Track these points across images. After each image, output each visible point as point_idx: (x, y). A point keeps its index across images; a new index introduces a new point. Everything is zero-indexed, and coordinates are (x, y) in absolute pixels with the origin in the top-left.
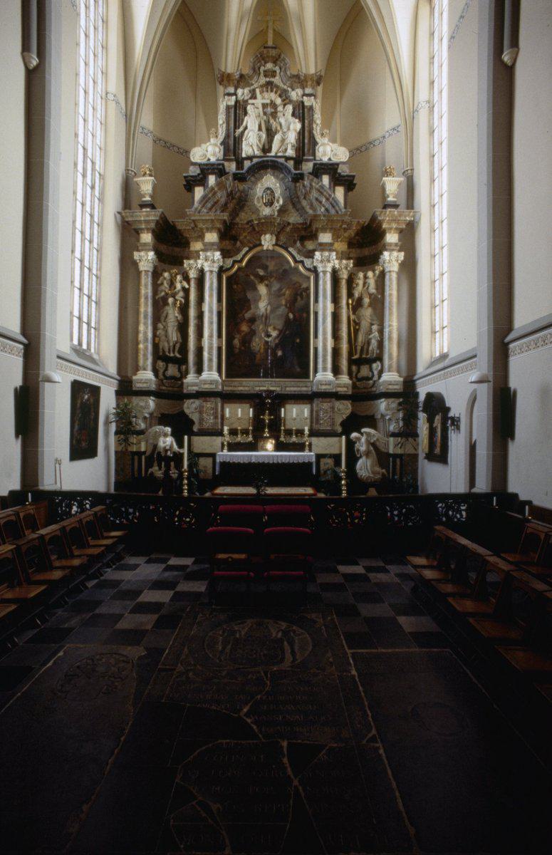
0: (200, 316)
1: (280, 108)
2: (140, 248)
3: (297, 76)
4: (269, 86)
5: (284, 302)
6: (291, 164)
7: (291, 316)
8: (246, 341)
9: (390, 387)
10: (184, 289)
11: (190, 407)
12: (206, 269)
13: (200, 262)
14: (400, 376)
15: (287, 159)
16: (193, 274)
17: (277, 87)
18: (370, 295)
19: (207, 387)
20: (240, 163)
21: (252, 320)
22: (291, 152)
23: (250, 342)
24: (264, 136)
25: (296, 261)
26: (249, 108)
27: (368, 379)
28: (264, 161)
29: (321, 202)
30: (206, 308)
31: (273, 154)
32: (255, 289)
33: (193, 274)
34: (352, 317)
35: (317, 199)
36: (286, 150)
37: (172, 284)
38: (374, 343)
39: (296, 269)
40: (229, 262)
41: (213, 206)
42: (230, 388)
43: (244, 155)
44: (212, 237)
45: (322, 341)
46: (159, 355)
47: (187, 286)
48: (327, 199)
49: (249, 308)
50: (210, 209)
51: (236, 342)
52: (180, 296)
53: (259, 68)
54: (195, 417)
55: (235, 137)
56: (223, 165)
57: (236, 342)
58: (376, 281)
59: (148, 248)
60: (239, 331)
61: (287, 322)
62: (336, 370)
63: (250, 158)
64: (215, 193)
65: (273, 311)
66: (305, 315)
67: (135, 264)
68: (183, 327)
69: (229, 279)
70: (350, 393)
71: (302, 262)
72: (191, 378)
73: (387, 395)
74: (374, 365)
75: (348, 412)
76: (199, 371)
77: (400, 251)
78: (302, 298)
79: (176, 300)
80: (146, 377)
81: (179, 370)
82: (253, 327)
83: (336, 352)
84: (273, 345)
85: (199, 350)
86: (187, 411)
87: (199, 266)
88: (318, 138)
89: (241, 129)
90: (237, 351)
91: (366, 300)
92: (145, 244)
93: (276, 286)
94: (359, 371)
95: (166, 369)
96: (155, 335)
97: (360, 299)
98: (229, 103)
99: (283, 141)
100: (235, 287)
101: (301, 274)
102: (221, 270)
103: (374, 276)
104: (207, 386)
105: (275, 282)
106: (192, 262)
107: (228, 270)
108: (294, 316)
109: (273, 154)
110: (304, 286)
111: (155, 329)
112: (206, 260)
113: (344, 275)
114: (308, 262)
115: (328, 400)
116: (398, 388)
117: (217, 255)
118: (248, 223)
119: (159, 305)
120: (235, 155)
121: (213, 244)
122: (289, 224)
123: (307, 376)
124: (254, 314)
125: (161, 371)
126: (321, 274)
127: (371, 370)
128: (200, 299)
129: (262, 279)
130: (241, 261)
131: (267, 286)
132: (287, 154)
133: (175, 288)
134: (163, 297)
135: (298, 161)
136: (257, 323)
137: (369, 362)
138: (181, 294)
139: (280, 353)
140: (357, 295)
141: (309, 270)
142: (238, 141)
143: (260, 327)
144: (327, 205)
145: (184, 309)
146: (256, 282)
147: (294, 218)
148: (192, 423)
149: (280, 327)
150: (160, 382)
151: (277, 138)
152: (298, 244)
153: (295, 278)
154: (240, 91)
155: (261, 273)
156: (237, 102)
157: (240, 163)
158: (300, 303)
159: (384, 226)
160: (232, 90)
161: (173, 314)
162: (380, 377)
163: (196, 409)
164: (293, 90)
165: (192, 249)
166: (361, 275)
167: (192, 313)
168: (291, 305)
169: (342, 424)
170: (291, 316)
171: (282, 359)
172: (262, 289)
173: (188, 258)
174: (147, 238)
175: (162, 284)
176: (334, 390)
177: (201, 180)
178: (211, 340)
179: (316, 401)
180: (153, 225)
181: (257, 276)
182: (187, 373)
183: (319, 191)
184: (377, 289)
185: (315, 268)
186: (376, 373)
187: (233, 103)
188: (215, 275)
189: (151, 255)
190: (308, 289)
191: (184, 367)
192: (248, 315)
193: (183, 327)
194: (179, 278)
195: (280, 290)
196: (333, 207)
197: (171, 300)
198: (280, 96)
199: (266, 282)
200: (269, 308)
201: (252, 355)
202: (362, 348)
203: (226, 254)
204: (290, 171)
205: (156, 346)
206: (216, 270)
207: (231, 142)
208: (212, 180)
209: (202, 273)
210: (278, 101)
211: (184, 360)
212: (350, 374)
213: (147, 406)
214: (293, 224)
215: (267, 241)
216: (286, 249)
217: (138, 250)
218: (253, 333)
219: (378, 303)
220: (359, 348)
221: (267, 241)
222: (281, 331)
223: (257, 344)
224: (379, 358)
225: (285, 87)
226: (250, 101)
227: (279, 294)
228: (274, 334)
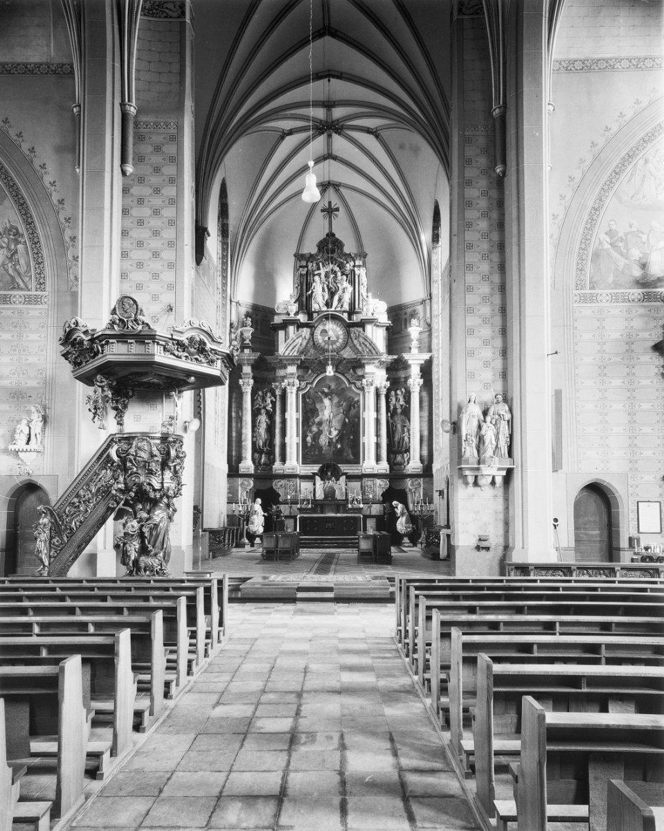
0: (284, 422)
1: (339, 274)
2: (243, 376)
3: (350, 255)
4: (333, 261)
5: (342, 411)
6: (345, 316)
7: (347, 420)
8: (316, 437)
9: (414, 470)
10: (272, 401)
11: (278, 485)
12: (288, 391)
13: (283, 384)
14: (422, 463)
15: (344, 312)
16: (278, 392)
17: (336, 260)
18: (402, 406)
19: (288, 472)
20: (310, 315)
21: (320, 424)
22: (346, 307)
23: (319, 438)
24: (327, 297)
25: (350, 383)
26: (317, 278)
27: (401, 464)
28: (328, 314)
29: (366, 346)
30: (287, 415)
31: (333, 309)
32: (322, 401)
33: (278, 392)
34: (391, 421)
35: (363, 343)
36: (342, 306)
37: (264, 400)
38: (406, 438)
39: (350, 389)
40: (303, 384)
41: (293, 348)
42: (305, 471)
43: (313, 310)
44: (292, 369)
45: (369, 439)
46: (255, 449)
47: (274, 400)
48: (370, 344)
49: (318, 415)
50: (291, 350)
51: (309, 439)
52: (269, 407)
53: (323, 248)
54: (281, 492)
55: (306, 297)
56: (299, 320)
57: (309, 439)
58: (404, 397)
59: (248, 376)
60: (311, 432)
61: (344, 424)
62: (378, 459)
63: (318, 312)
64: (294, 341)
65: (334, 417)
66: (356, 420)
67: (239, 387)
68: (270, 429)
69: (304, 396)
70: (388, 472)
71: (354, 383)
72: (277, 466)
73: (412, 476)
74: (405, 455)
75: (388, 486)
76: (283, 460)
77: (421, 378)
78: (354, 408)
79: (267, 410)
80: (247, 465)
81: (269, 459)
82: (320, 428)
83: (378, 446)
84: (334, 440)
85: (283, 446)
86: (274, 487)
87: (283, 387)
88: (365, 294)
89: (310, 292)
90: (309, 445)
91: (399, 411)
92: (246, 374)
93: (336, 400)
94: (395, 458)
95: (261, 459)
96: (253, 437)
97: (395, 409)
98: (302, 273)
99: (340, 300)
100: (308, 400)
101: (353, 391)
102: (299, 389)
103: (402, 392)
104: (290, 471)
105: (336, 397)
106: (277, 384)
107: (303, 389)
108: (349, 420)
109: (333, 309)
110: (356, 399)
111: (253, 431)
112: (289, 385)
113: (384, 392)
114: (358, 383)
115: (372, 479)
116: (419, 471)
117: (297, 382)
118: (316, 359)
119: (255, 413)
120: (306, 309)
121: (292, 374)
122: (345, 359)
123: (359, 464)
124: (321, 419)
125: (257, 461)
126: (367, 393)
127: (403, 458)
128: (284, 410)
129: (326, 395)
130: (312, 383)
131: (330, 399)
132: (343, 309)
133: (266, 402)
134: (257, 409)
135: (352, 312)
136: (323, 425)
137: (402, 453)
138: (270, 406)
139: (339, 446)
140: (392, 407)
141: (359, 389)
142: (309, 298)
143: (325, 428)
144: (371, 348)
145: (271, 416)
146: (323, 397)
147: (347, 354)
148: (279, 496)
149: (339, 428)
150: (256, 469)
151: (336, 298)
152: (351, 371)
153: (349, 394)
154: (310, 265)
155: (326, 390)
156: (307, 272)
157: (310, 315)
158: (353, 411)
159: (410, 362)
160: (304, 263)
161: (263, 418)
162: (408, 463)
163: (281, 486)
164: (347, 262)
165: (277, 374)
166: (393, 393)
167: (278, 419)
168: (347, 413)
169: (383, 495)
170: (347, 420)
171: (341, 451)
172: (327, 402)
173: (275, 382)
174: (247, 369)
175: (257, 398)
176: (376, 472)
177: (284, 325)
178: (293, 440)
179: (365, 480)
180: (252, 362)
181: (323, 392)
182: (273, 461)
183: (364, 339)
184: (405, 402)
185: (363, 388)
186: (406, 460)
187: (305, 272)
188: (294, 396)
189: (252, 381)
190: (358, 401)
191: (272, 457)
192: (317, 420)
193: (270, 429)
194: (269, 394)
195: (339, 402)
196: (374, 349)
197: (263, 411)
198: (338, 266)
199: (330, 397)
200: (332, 414)
201: (321, 448)
202: (399, 442)
203: (300, 378)
204: (345, 321)
205: (254, 444)
206: (294, 390)
207: (304, 300)
208: (291, 329)
209: (284, 392)
210: (337, 269)
211: (271, 453)
212: (389, 460)
213: (249, 484)
214: (348, 359)
215: (330, 371)
216: (343, 375)
217: (242, 379)
218: (320, 433)
219: (406, 412)
220: (396, 443)
221: (330, 371)
222: (339, 431)
223: (323, 440)
224: (408, 450)
225: (342, 260)
226: (316, 273)
227: (339, 405)
228: (335, 433)
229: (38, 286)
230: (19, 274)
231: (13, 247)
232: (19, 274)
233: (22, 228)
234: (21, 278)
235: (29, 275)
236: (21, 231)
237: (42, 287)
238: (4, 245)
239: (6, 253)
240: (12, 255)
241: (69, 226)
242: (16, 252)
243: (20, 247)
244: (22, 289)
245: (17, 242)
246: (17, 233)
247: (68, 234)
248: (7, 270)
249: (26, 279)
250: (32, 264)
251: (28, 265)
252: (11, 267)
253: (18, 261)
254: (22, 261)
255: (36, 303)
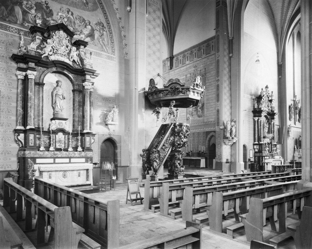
229: (112, 53)
230: (104, 45)
231: (102, 32)
232: (104, 45)
233: (105, 25)
234: (105, 46)
235: (108, 46)
236: (105, 26)
237: (114, 53)
238: (98, 30)
239: (99, 34)
240: (102, 35)
241: (123, 30)
242: (103, 35)
243: (104, 32)
244: (105, 52)
245: (103, 30)
246: (103, 26)
247: (123, 33)
248: (99, 42)
249: (107, 48)
250: (110, 42)
251: (108, 42)
252: (101, 41)
253: (104, 39)
254: (105, 39)
255: (112, 60)
